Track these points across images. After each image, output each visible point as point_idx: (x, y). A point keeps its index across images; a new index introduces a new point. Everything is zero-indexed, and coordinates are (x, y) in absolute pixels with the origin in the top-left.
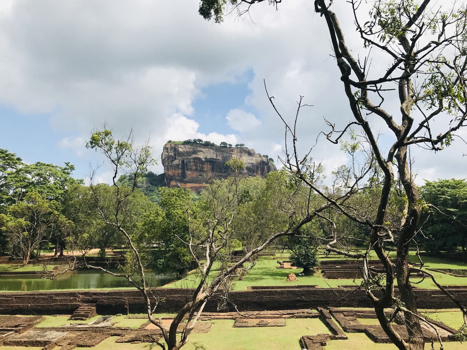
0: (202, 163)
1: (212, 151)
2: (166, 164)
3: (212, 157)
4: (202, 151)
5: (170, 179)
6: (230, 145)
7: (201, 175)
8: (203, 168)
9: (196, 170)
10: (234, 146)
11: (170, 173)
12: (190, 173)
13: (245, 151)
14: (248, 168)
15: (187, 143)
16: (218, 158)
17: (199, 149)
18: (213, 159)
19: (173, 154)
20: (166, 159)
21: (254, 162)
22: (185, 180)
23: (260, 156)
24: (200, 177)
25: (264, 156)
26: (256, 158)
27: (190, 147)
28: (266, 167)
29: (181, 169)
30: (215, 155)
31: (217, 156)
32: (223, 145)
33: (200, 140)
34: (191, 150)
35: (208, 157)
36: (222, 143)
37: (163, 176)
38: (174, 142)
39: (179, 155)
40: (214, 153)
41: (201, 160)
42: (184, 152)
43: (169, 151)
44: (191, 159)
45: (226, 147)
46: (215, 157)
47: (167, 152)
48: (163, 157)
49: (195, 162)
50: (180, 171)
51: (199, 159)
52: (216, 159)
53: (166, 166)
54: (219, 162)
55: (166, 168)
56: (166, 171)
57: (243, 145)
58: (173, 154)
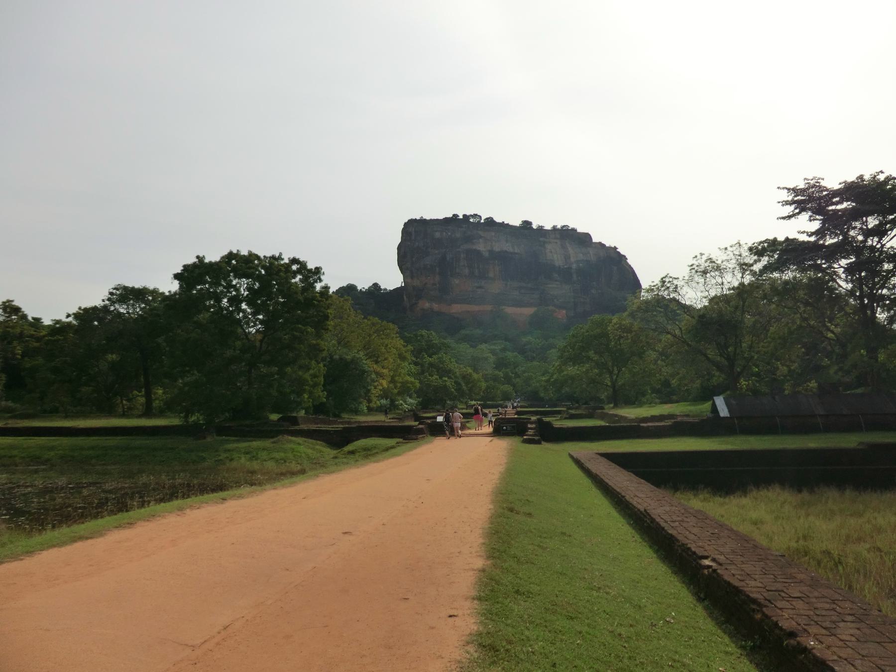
3: (505, 249)
4: (481, 237)
11: (416, 283)
12: (457, 281)
18: (506, 251)
43: (413, 238)
52: (511, 253)
56: (409, 280)
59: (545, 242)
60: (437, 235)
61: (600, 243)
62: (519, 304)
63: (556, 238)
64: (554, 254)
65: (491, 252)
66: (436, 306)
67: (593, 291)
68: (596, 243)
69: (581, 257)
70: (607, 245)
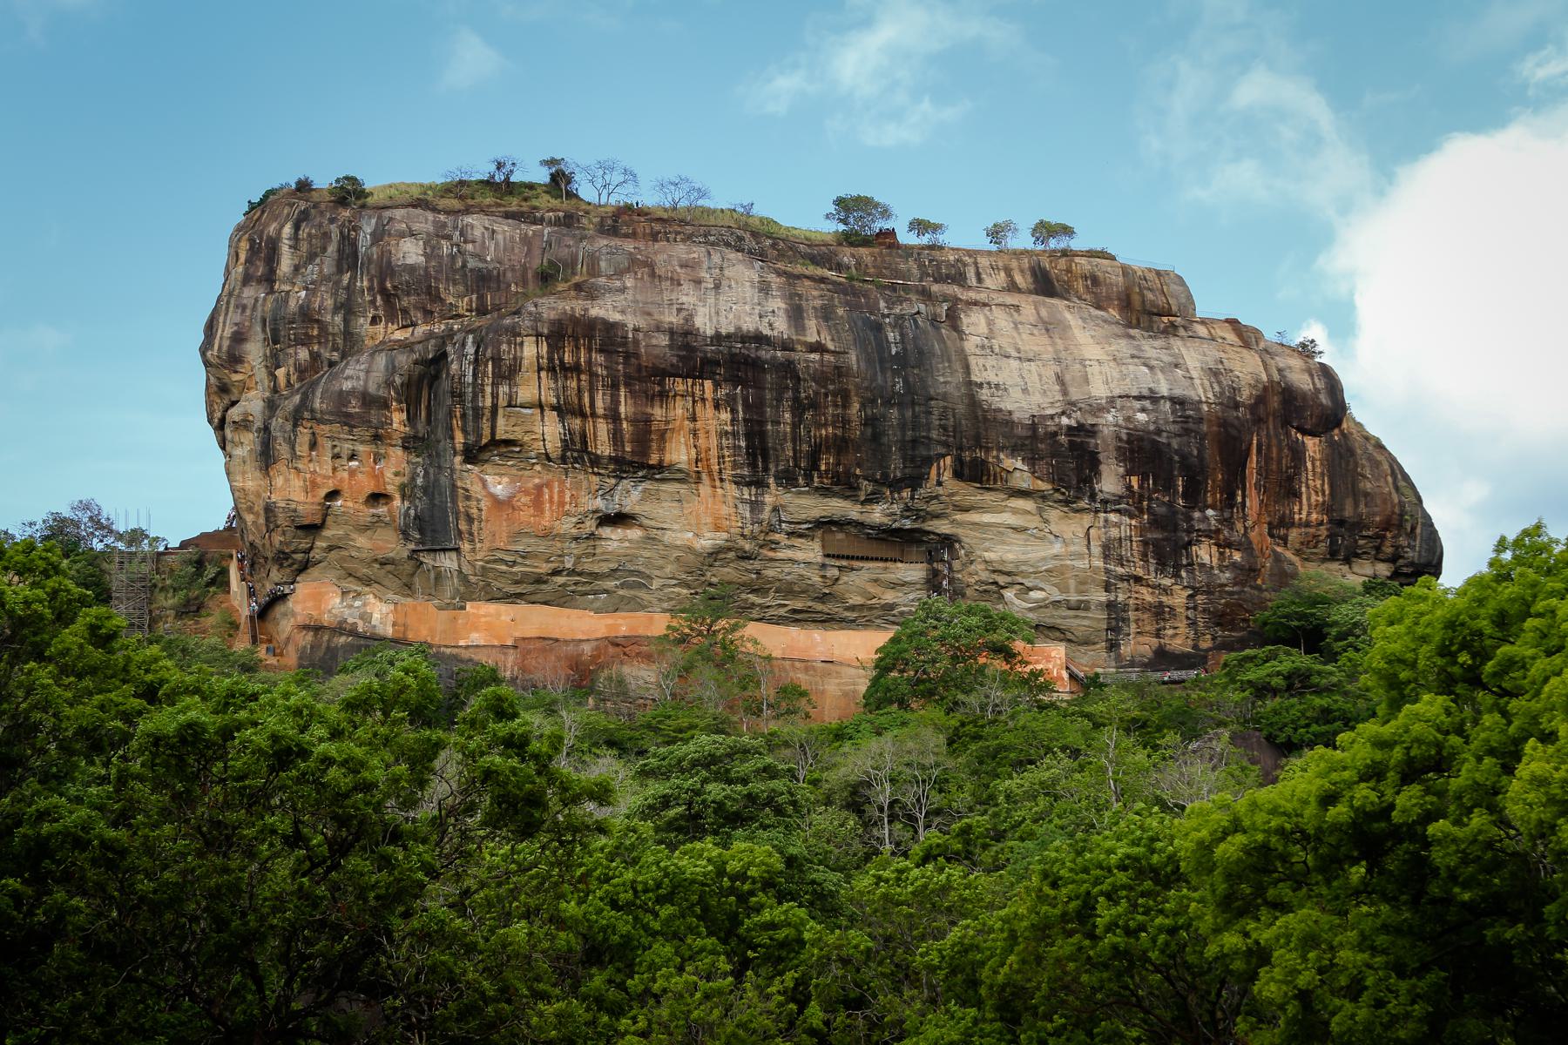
2: (252, 404)
5: (282, 558)
7: (620, 519)
8: (646, 435)
9: (576, 452)
11: (292, 490)
18: (759, 339)
19: (325, 300)
20: (255, 351)
21: (1201, 391)
22: (448, 562)
23: (1246, 336)
24: (614, 538)
26: (1212, 353)
28: (1312, 446)
30: (777, 304)
31: (796, 315)
35: (705, 323)
37: (203, 560)
39: (392, 310)
40: (764, 288)
43: (285, 264)
46: (780, 326)
48: (225, 331)
49: (557, 369)
51: (608, 337)
52: (787, 346)
53: (244, 425)
55: (247, 444)
56: (252, 481)
57: (1067, 231)
60: (411, 252)
61: (1233, 323)
62: (820, 610)
63: (1012, 287)
65: (684, 337)
66: (379, 612)
67: (1205, 553)
68: (1203, 322)
69: (1141, 379)
70: (1270, 335)
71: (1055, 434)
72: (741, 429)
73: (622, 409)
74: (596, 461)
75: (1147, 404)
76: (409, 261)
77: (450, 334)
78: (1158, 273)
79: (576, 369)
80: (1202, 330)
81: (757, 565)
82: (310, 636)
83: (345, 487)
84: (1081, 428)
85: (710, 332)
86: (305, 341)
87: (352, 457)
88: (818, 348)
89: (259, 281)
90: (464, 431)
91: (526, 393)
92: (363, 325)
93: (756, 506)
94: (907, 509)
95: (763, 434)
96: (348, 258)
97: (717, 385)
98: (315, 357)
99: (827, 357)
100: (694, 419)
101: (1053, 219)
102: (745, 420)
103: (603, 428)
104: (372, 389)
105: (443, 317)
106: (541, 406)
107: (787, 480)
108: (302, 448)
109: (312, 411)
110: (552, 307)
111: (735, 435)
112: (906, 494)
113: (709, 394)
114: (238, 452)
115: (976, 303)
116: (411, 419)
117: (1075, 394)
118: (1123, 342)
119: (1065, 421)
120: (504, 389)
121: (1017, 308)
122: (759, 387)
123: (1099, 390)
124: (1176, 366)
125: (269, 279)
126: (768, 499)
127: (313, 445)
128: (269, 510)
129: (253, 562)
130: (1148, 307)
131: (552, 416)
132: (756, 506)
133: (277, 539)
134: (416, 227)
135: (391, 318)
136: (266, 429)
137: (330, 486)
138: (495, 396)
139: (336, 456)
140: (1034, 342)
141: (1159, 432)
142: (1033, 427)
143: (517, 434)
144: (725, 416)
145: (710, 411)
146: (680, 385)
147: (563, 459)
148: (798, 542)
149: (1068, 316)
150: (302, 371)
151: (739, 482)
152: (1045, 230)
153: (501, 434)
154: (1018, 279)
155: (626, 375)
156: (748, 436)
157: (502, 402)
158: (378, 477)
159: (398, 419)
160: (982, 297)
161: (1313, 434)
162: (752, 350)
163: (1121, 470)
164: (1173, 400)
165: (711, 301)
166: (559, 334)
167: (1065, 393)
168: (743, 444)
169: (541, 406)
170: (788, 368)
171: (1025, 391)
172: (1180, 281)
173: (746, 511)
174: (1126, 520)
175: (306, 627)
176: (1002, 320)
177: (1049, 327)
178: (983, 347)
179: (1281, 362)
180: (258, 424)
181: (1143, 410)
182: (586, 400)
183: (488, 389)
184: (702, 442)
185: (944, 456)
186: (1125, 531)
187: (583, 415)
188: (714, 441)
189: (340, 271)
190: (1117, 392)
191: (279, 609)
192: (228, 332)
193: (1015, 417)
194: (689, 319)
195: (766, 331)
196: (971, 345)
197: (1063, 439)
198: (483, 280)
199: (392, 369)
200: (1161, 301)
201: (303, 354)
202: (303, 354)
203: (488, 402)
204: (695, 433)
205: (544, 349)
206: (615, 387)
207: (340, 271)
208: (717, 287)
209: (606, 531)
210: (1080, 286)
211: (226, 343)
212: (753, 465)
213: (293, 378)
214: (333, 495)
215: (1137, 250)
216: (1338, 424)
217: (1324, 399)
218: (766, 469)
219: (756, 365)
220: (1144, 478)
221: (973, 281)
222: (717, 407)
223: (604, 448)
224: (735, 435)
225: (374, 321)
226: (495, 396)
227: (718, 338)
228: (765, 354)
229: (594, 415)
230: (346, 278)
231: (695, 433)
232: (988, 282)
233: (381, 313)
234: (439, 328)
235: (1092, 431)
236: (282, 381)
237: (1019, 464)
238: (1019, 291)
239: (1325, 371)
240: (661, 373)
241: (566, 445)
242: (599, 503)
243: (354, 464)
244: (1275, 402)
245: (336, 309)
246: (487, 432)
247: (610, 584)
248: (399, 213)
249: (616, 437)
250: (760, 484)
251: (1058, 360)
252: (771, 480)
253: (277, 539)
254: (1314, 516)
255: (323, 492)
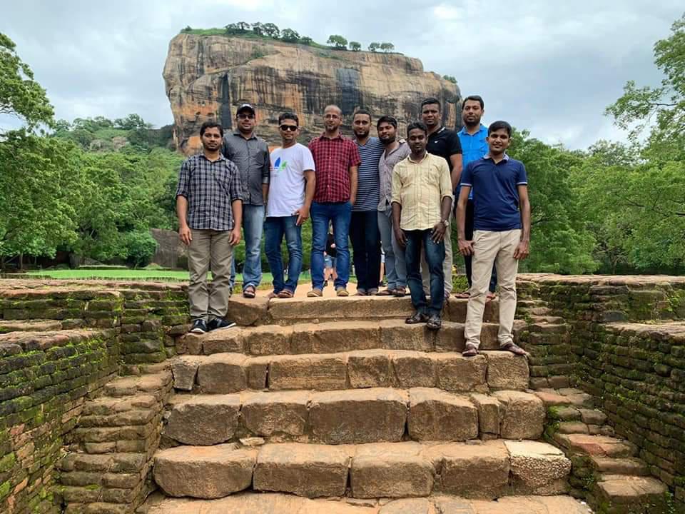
0: (280, 83)
1: (305, 53)
2: (176, 89)
3: (308, 69)
5: (186, 130)
6: (356, 45)
8: (280, 98)
10: (365, 47)
11: (188, 113)
13: (398, 60)
14: (408, 106)
15: (234, 31)
16: (325, 72)
17: (268, 47)
18: (310, 73)
19: (194, 61)
20: (177, 74)
23: (437, 77)
25: (446, 78)
27: (242, 41)
28: (452, 106)
29: (218, 100)
30: (315, 64)
31: (320, 66)
32: (334, 45)
33: (271, 28)
34: (247, 49)
35: (296, 69)
36: (332, 39)
37: (167, 132)
38: (199, 32)
39: (213, 63)
40: (312, 59)
41: (277, 76)
42: (228, 53)
43: (184, 51)
44: (245, 70)
45: (344, 49)
46: (316, 70)
47: (180, 55)
48: (169, 69)
49: (257, 80)
50: (215, 106)
51: (270, 71)
53: (174, 94)
54: (327, 84)
55: (177, 98)
56: (177, 110)
57: (390, 46)
58: (194, 61)
59: (361, 65)
60: (216, 48)
61: (432, 72)
64: (375, 83)
65: (289, 72)
71: (386, 101)
72: (305, 98)
73: (274, 92)
74: (267, 105)
75: (411, 94)
76: (217, 50)
77: (228, 71)
78: (415, 59)
79: (262, 80)
80: (425, 75)
81: (310, 135)
82: (193, 151)
83: (201, 110)
84: (394, 100)
85: (297, 71)
86: (190, 72)
87: (203, 103)
88: (326, 76)
89: (177, 55)
90: (233, 97)
91: (248, 87)
92: (205, 68)
93: (309, 119)
94: (348, 120)
95: (311, 99)
96: (201, 49)
97: (299, 86)
98: (193, 77)
99: (328, 79)
100: (293, 95)
101: (387, 42)
102: (307, 96)
103: (269, 97)
104: (208, 85)
105: (226, 66)
106: (253, 90)
107: (317, 112)
108: (190, 101)
109: (192, 90)
110: (255, 63)
111: (303, 99)
112: (348, 116)
113: (297, 88)
114: (174, 102)
115: (366, 66)
116: (219, 92)
117: (393, 90)
118: (405, 77)
119: (389, 97)
120: (243, 85)
121: (378, 67)
122: (310, 86)
123: (398, 89)
124: (418, 83)
125: (180, 55)
126: (313, 117)
127: (193, 100)
128: (182, 117)
129: (178, 132)
130: (410, 67)
131: (255, 93)
132: (309, 119)
133: (184, 125)
134: (219, 41)
135: (212, 66)
136: (180, 96)
137: (197, 111)
138: (240, 87)
139: (199, 103)
140: (382, 77)
141: (413, 101)
142: (381, 99)
143: (247, 97)
144: (301, 94)
145: (297, 93)
146: (289, 85)
147: (259, 105)
148: (320, 129)
149: (391, 69)
150: (189, 81)
151: (305, 112)
152: (384, 46)
153: (242, 98)
154: (378, 60)
155: (276, 82)
156: (308, 100)
157: (242, 89)
158: (210, 108)
159: (215, 94)
160: (368, 63)
161: (452, 103)
162: (308, 76)
163: (403, 111)
164: (417, 93)
165: (298, 62)
166: (257, 71)
167: (390, 90)
168: (306, 102)
169: (253, 90)
170: (317, 82)
171: (379, 89)
172: (420, 61)
173: (307, 120)
174: (404, 124)
175: (192, 148)
176: (374, 71)
177: (387, 73)
178: (368, 77)
179: (445, 84)
180: (178, 94)
181: (410, 95)
182: (265, 89)
183: (239, 85)
184: (295, 101)
185: (357, 106)
186: (403, 127)
187: (264, 93)
188: (298, 101)
189: (199, 53)
190: (403, 90)
191: (185, 144)
192: (170, 69)
193: (377, 96)
194: (291, 68)
195: (311, 70)
196: (365, 75)
197: (388, 102)
198: (237, 54)
199: (213, 79)
200: (415, 66)
201: (189, 75)
202: (189, 75)
203: (239, 89)
204: (293, 99)
205: (253, 75)
206: (272, 85)
207: (199, 53)
208: (299, 59)
209: (271, 125)
210: (394, 62)
211: (169, 72)
212: (308, 108)
213: (187, 82)
214: (199, 113)
215: (410, 53)
216: (459, 100)
217: (455, 94)
218: (312, 109)
219: (309, 80)
220: (409, 113)
221: (366, 59)
222: (299, 91)
223: (270, 102)
224: (303, 99)
225: (208, 66)
226: (240, 87)
227: (299, 72)
228: (312, 77)
229: (267, 93)
230: (200, 55)
231: (293, 99)
232: (370, 60)
233: (210, 64)
234: (225, 69)
235: (396, 100)
236: (184, 83)
237: (377, 108)
238: (377, 62)
239: (456, 86)
240: (285, 82)
241: (260, 101)
242: (269, 117)
243: (203, 105)
244: (442, 94)
245: (197, 64)
246: (238, 96)
247: (272, 139)
248: (213, 37)
249: (273, 99)
250: (310, 113)
251: (388, 81)
252: (313, 112)
253: (184, 125)
254: (451, 125)
255: (196, 112)
